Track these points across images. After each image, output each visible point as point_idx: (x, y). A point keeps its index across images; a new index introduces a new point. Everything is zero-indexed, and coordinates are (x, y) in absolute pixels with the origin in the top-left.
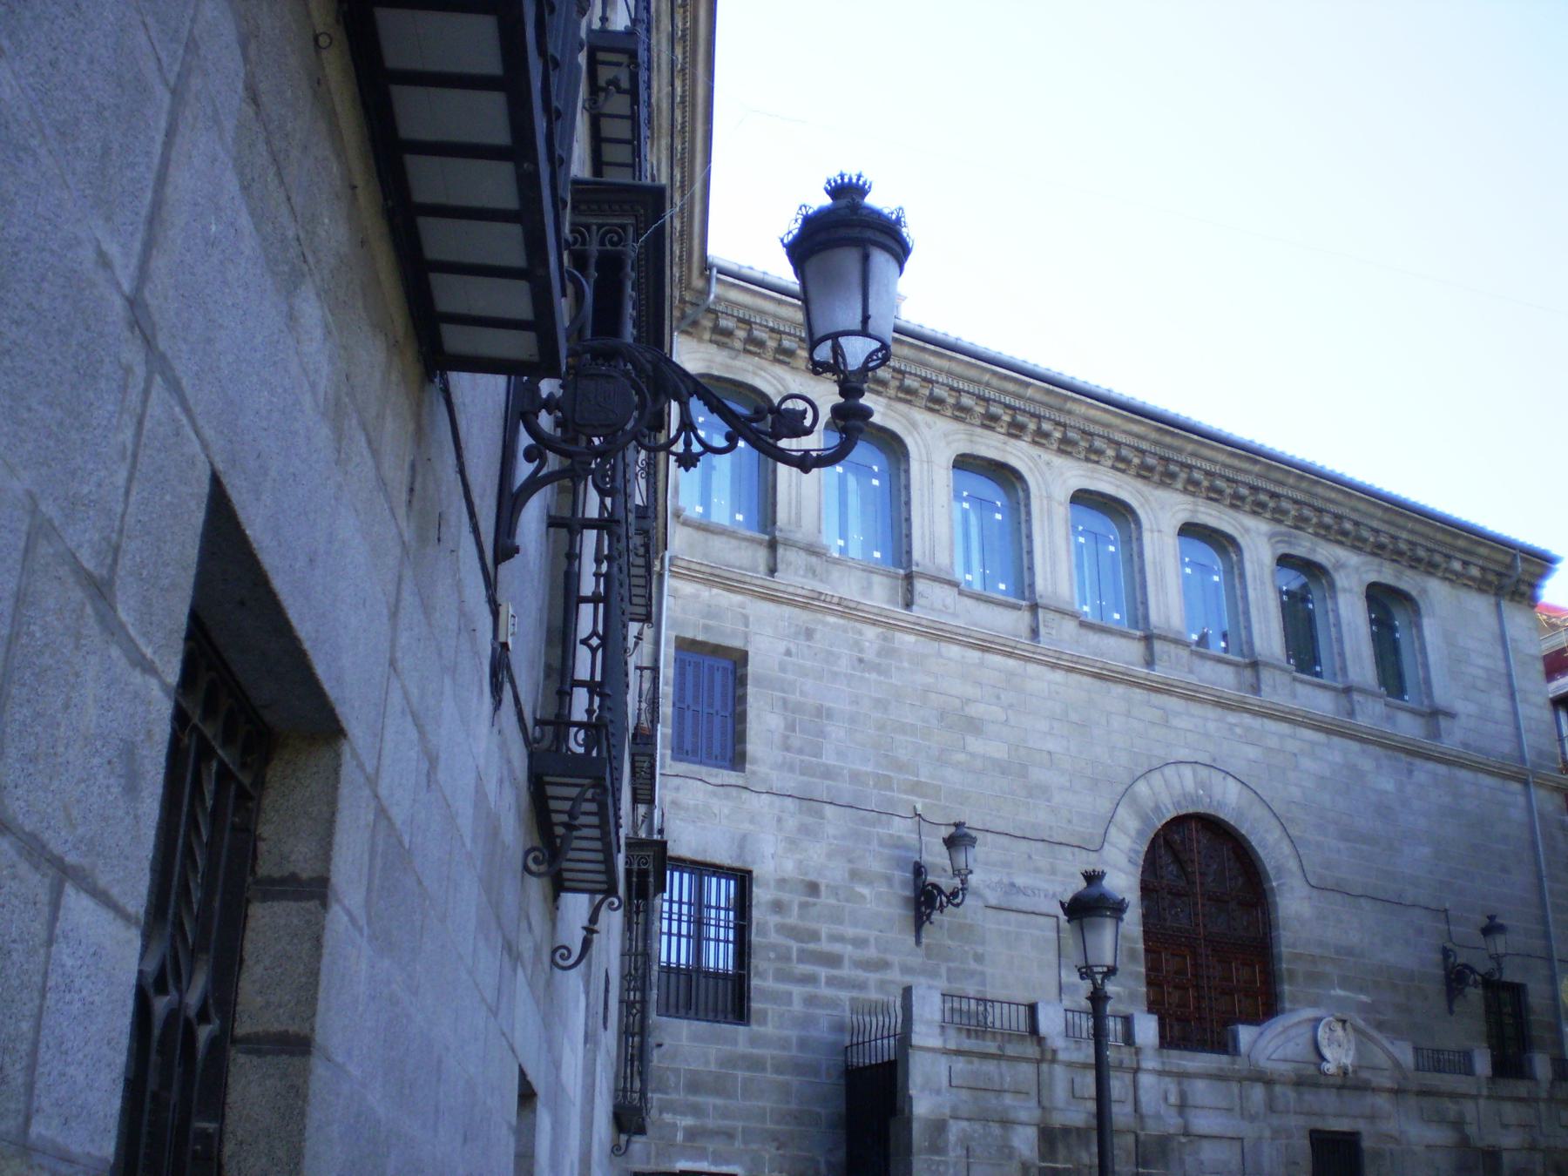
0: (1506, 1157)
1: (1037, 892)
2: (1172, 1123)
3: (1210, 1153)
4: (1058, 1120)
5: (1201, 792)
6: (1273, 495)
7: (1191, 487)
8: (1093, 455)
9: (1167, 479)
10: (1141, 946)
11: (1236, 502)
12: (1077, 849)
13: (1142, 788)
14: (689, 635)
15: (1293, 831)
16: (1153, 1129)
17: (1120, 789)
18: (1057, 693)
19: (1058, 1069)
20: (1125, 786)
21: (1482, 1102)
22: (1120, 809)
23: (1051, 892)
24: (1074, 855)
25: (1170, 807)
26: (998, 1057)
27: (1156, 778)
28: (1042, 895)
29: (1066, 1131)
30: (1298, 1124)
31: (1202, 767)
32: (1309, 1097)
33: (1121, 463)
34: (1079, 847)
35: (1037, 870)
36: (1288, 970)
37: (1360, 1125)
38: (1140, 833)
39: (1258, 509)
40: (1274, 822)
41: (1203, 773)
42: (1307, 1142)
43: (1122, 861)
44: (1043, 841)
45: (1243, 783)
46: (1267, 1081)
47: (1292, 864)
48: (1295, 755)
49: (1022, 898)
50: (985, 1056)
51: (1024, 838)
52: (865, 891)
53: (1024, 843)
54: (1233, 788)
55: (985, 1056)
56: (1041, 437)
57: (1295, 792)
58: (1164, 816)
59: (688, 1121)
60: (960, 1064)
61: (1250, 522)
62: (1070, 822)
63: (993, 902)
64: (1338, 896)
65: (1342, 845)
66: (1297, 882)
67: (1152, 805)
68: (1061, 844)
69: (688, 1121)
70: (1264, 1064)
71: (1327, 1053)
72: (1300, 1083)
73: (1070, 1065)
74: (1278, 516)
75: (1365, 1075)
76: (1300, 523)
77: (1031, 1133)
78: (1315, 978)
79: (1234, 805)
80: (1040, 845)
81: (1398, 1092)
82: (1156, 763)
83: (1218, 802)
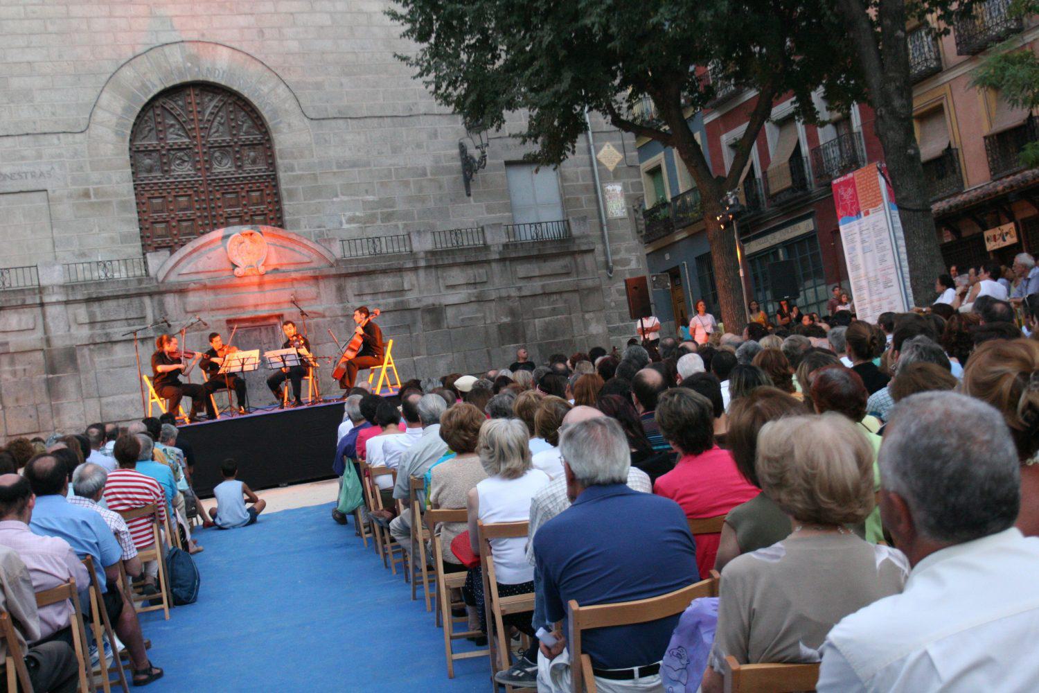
0: (450, 313)
1: (24, 175)
5: (189, 65)
12: (61, 135)
13: (127, 73)
15: (291, 78)
16: (58, 343)
17: (104, 78)
18: (34, 13)
20: (108, 76)
21: (422, 273)
22: (105, 97)
23: (38, 172)
24: (59, 139)
25: (157, 82)
28: (29, 176)
31: (191, 44)
34: (64, 132)
35: (23, 158)
36: (287, 190)
38: (126, 110)
40: (268, 73)
41: (192, 49)
43: (111, 136)
44: (27, 134)
45: (233, 48)
47: (290, 105)
48: (292, 14)
49: (9, 182)
51: (8, 136)
53: (10, 139)
57: (293, 45)
58: (150, 91)
62: (53, 114)
64: (341, 122)
65: (345, 80)
66: (296, 120)
67: (138, 84)
68: (45, 133)
71: (238, 261)
78: (316, 192)
79: (225, 68)
80: (25, 138)
82: (140, 49)
83: (208, 69)
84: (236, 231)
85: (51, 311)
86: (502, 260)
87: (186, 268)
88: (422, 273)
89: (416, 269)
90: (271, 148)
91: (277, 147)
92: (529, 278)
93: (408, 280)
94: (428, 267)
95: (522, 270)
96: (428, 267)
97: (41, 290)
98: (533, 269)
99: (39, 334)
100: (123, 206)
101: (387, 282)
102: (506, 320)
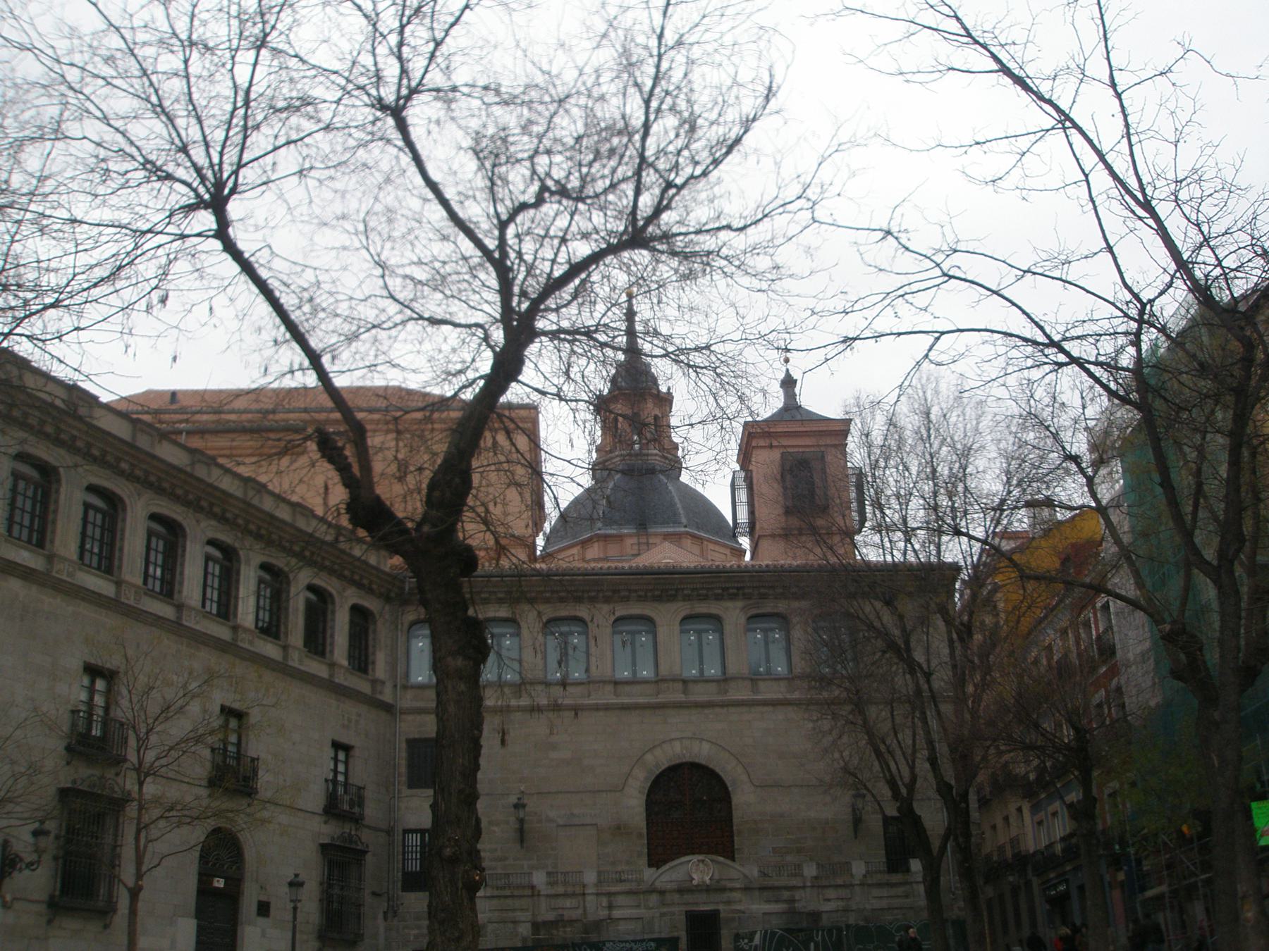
0: (824, 916)
2: (603, 913)
3: (622, 927)
4: (540, 919)
6: (738, 589)
7: (687, 598)
8: (625, 599)
9: (672, 598)
10: (645, 831)
11: (718, 598)
13: (649, 757)
14: (411, 736)
16: (591, 918)
19: (543, 899)
21: (808, 890)
26: (512, 896)
27: (658, 752)
29: (545, 923)
30: (678, 911)
32: (688, 898)
33: (642, 599)
37: (721, 907)
39: (733, 597)
42: (683, 917)
46: (662, 893)
47: (744, 777)
50: (506, 897)
52: (496, 829)
54: (706, 746)
55: (506, 897)
56: (593, 600)
59: (415, 932)
60: (495, 902)
61: (730, 604)
63: (561, 822)
69: (415, 932)
70: (658, 885)
71: (695, 876)
72: (681, 891)
73: (547, 896)
74: (747, 597)
75: (723, 883)
76: (763, 596)
77: (529, 925)
81: (746, 889)
84: (695, 858)
85: (589, 898)
86: (862, 884)
87: (665, 878)
88: (808, 890)
89: (804, 887)
90: (730, 803)
91: (734, 802)
92: (881, 898)
93: (798, 895)
94: (813, 887)
95: (876, 892)
96: (813, 887)
97: (584, 886)
98: (884, 892)
99: (580, 911)
100: (640, 835)
101: (786, 894)
102: (862, 923)
